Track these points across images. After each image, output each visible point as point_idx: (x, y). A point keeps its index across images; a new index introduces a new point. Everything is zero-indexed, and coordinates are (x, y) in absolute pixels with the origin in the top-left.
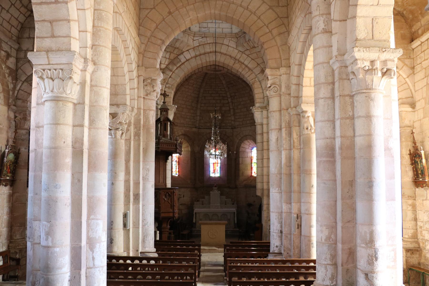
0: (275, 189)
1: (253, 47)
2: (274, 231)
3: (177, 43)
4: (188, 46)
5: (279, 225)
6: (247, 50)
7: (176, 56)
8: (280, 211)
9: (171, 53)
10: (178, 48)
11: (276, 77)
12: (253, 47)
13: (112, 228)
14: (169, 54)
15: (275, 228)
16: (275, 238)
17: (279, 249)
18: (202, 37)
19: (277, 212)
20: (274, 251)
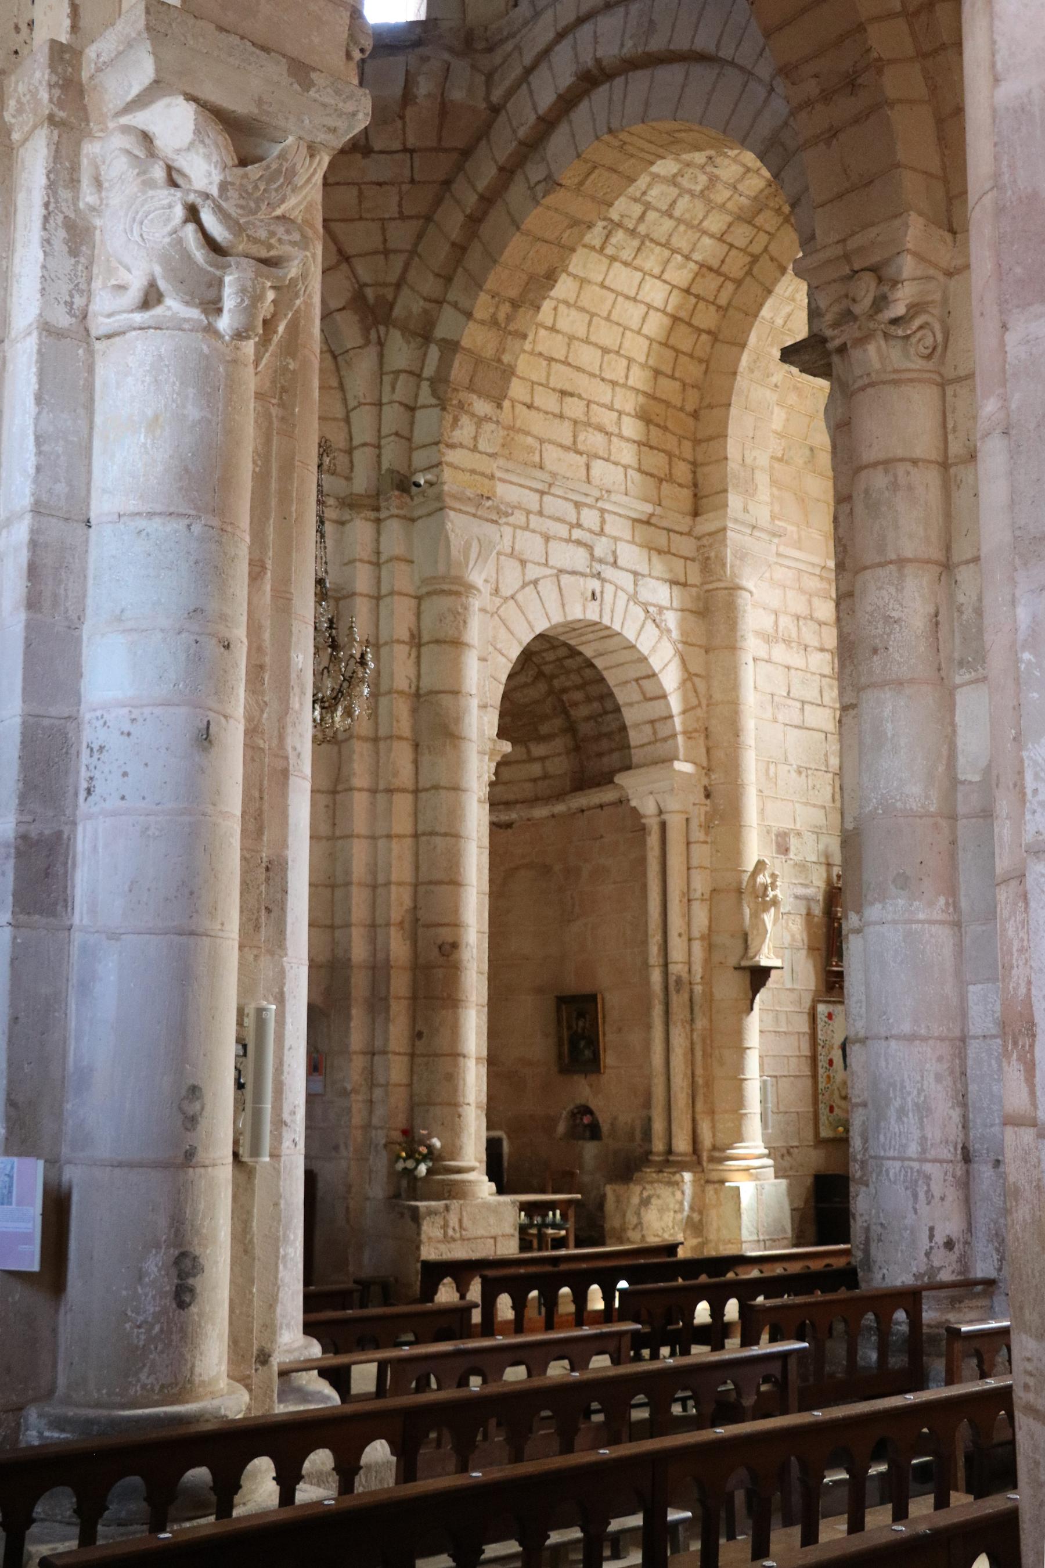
0: (931, 904)
2: (932, 1154)
5: (956, 1115)
8: (957, 1033)
11: (931, 272)
13: (190, 1154)
15: (934, 1133)
16: (937, 1190)
17: (959, 1260)
19: (941, 1039)
20: (932, 1271)
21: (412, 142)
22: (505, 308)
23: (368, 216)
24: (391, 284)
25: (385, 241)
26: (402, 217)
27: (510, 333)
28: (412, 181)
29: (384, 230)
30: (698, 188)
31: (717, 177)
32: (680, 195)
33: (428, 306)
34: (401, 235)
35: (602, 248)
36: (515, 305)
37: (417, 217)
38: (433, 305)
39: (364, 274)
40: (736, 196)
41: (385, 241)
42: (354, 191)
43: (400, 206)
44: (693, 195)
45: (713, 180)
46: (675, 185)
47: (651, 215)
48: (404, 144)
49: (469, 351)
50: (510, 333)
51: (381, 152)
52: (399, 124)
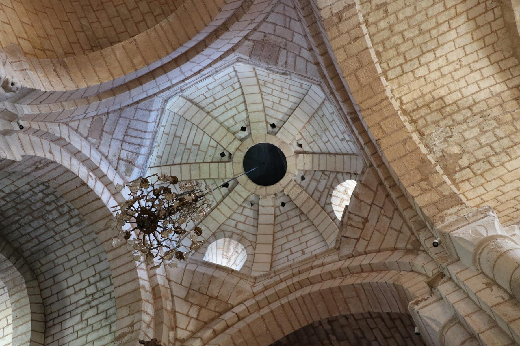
1: (364, 224)
3: (212, 287)
4: (240, 292)
6: (358, 239)
7: (213, 314)
9: (201, 307)
10: (216, 298)
12: (364, 224)
14: (195, 309)
18: (271, 278)
21: (369, 202)
22: (424, 184)
23: (386, 232)
24: (410, 236)
25: (396, 230)
26: (391, 219)
27: (437, 187)
28: (382, 208)
29: (392, 228)
30: (495, 124)
31: (496, 117)
32: (493, 132)
33: (414, 219)
34: (397, 223)
35: (493, 167)
36: (425, 179)
37: (394, 212)
38: (415, 217)
39: (401, 245)
40: (513, 113)
41: (396, 230)
42: (376, 232)
43: (387, 217)
44: (498, 128)
45: (495, 118)
46: (486, 132)
47: (495, 145)
48: (369, 205)
49: (426, 205)
50: (437, 187)
51: (368, 215)
52: (362, 203)
